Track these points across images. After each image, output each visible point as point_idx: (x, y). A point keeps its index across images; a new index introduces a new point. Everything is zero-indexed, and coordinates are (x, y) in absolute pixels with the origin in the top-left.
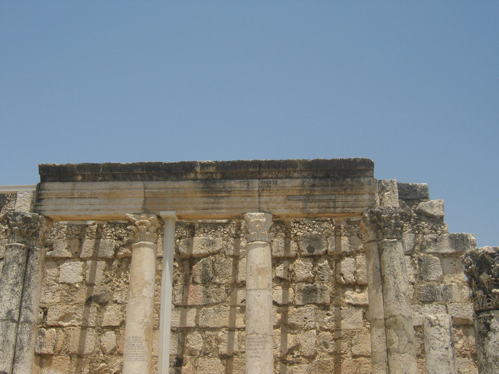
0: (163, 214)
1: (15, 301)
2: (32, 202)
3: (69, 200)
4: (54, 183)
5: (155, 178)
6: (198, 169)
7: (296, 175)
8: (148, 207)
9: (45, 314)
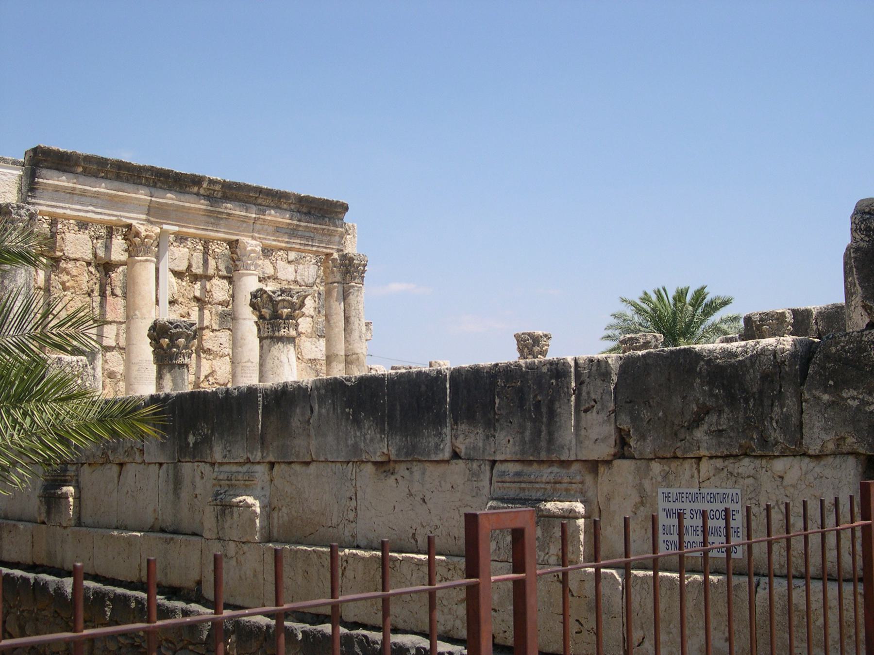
0: (165, 227)
2: (20, 190)
3: (68, 195)
4: (53, 171)
5: (159, 185)
6: (205, 185)
7: (285, 206)
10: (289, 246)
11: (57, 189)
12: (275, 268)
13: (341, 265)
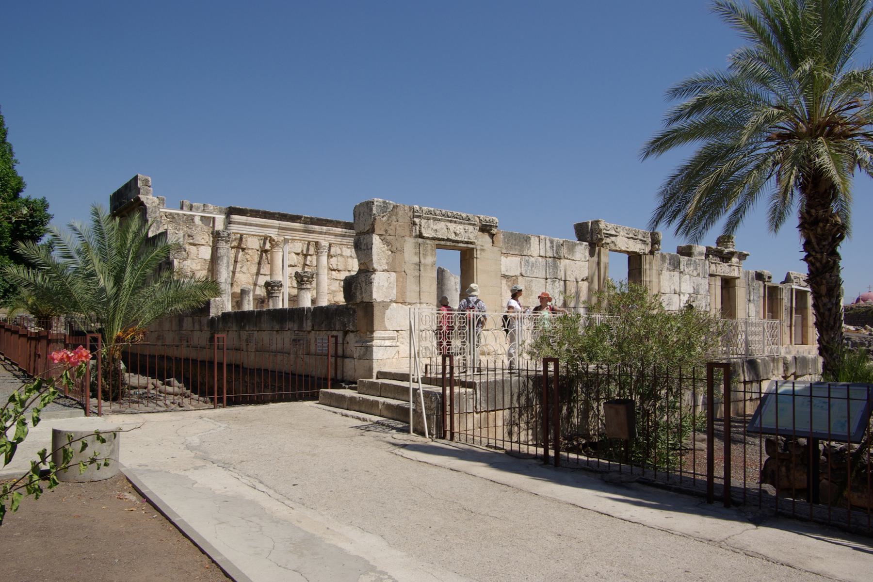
11: (239, 223)
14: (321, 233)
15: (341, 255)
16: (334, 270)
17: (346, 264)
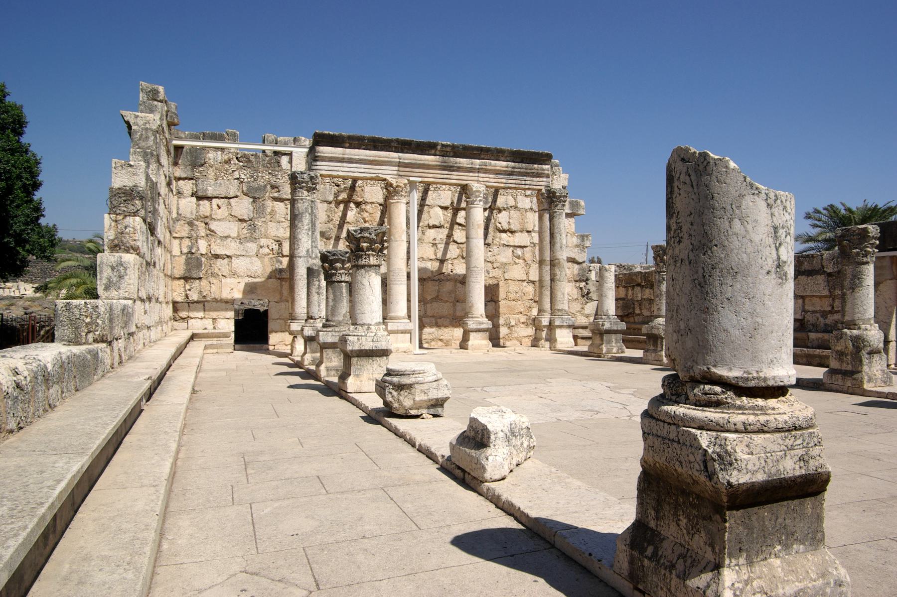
0: (412, 179)
1: (310, 242)
2: (307, 162)
3: (339, 164)
6: (439, 147)
8: (401, 173)
9: (280, 245)
10: (507, 185)
11: (331, 159)
12: (516, 201)
13: (548, 197)
14: (471, 170)
15: (516, 207)
16: (504, 231)
17: (523, 222)
